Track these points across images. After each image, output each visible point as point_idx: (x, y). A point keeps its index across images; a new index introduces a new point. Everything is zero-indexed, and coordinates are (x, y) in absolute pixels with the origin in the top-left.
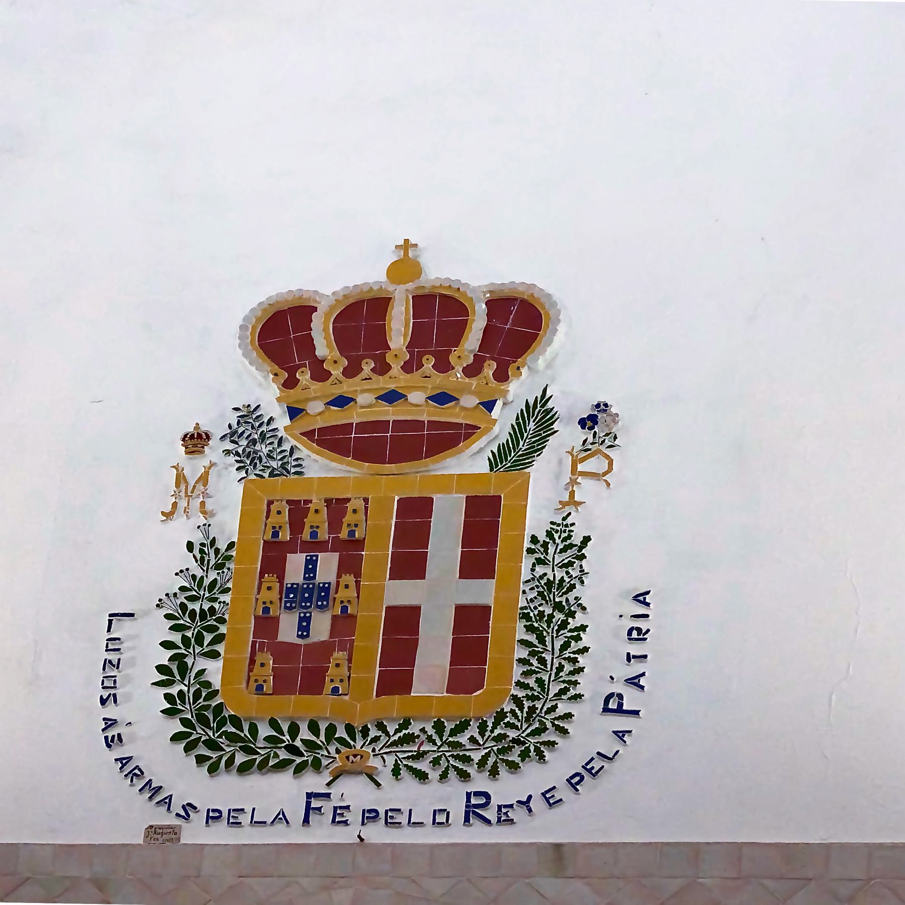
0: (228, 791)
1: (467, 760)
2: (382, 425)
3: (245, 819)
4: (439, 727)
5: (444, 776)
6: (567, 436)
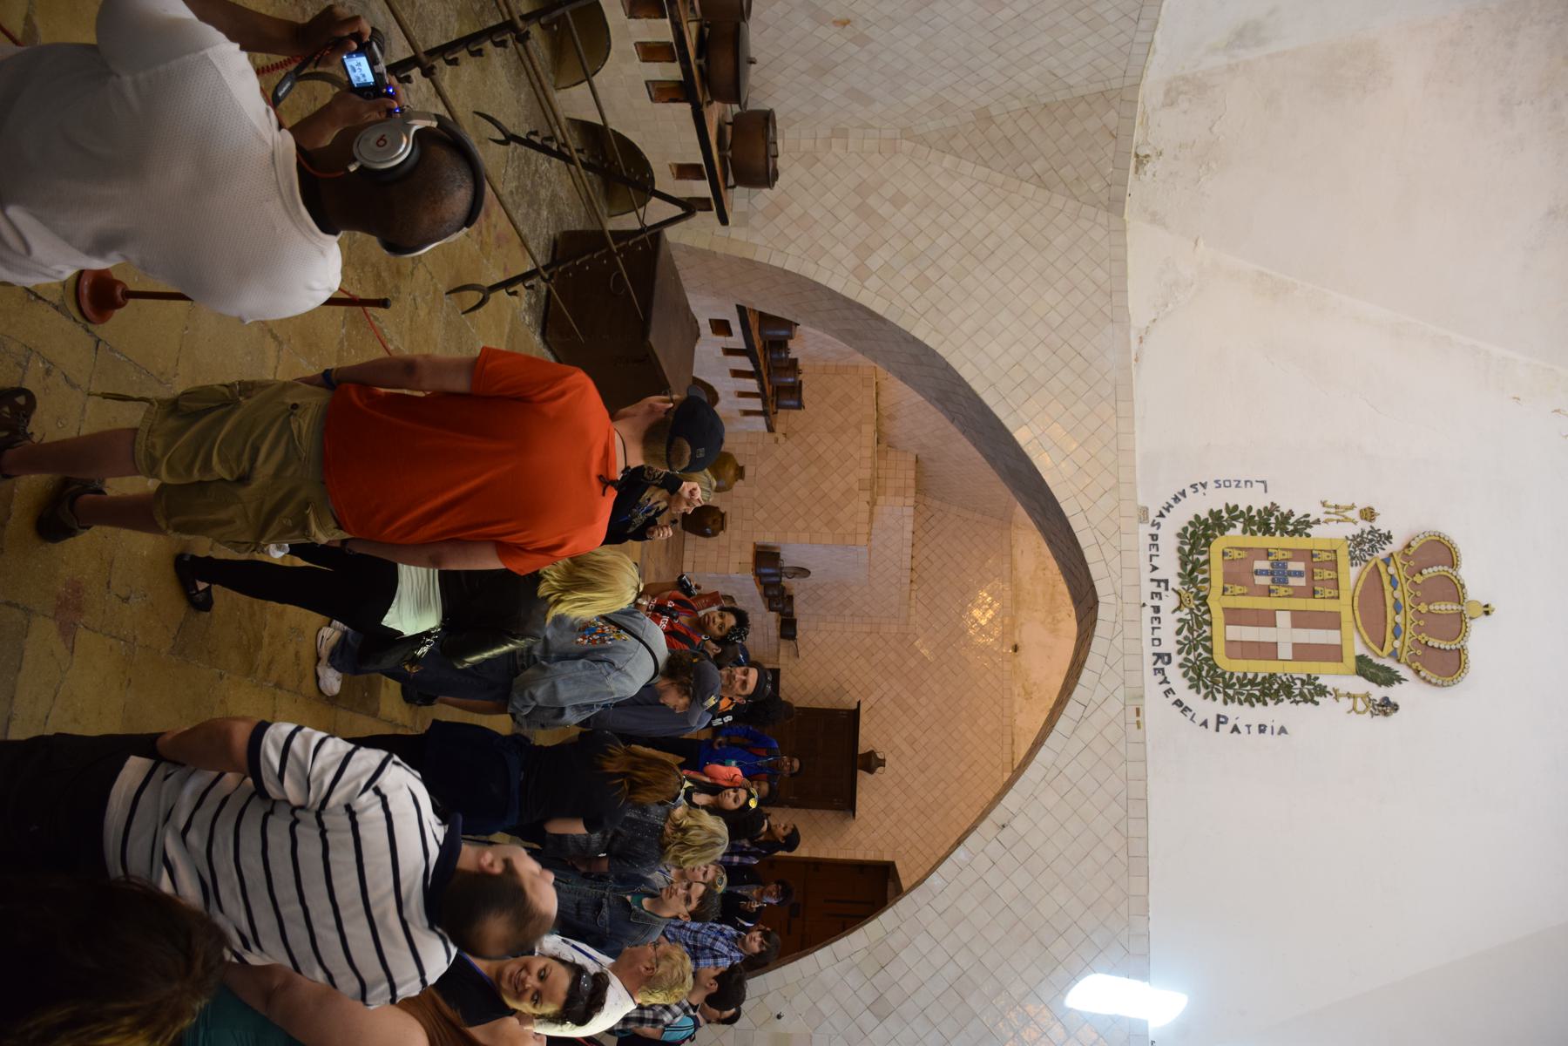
5: (1178, 642)
6: (1378, 692)
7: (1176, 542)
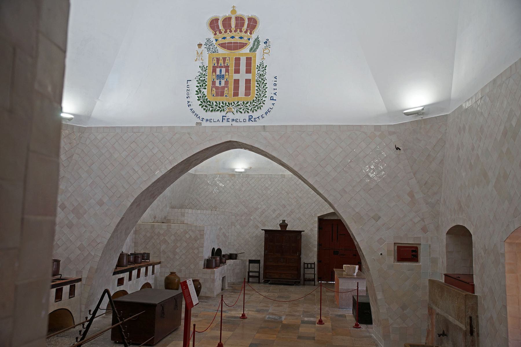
0: (209, 115)
1: (248, 109)
2: (231, 43)
3: (212, 121)
4: (244, 103)
6: (262, 45)
7: (209, 113)
